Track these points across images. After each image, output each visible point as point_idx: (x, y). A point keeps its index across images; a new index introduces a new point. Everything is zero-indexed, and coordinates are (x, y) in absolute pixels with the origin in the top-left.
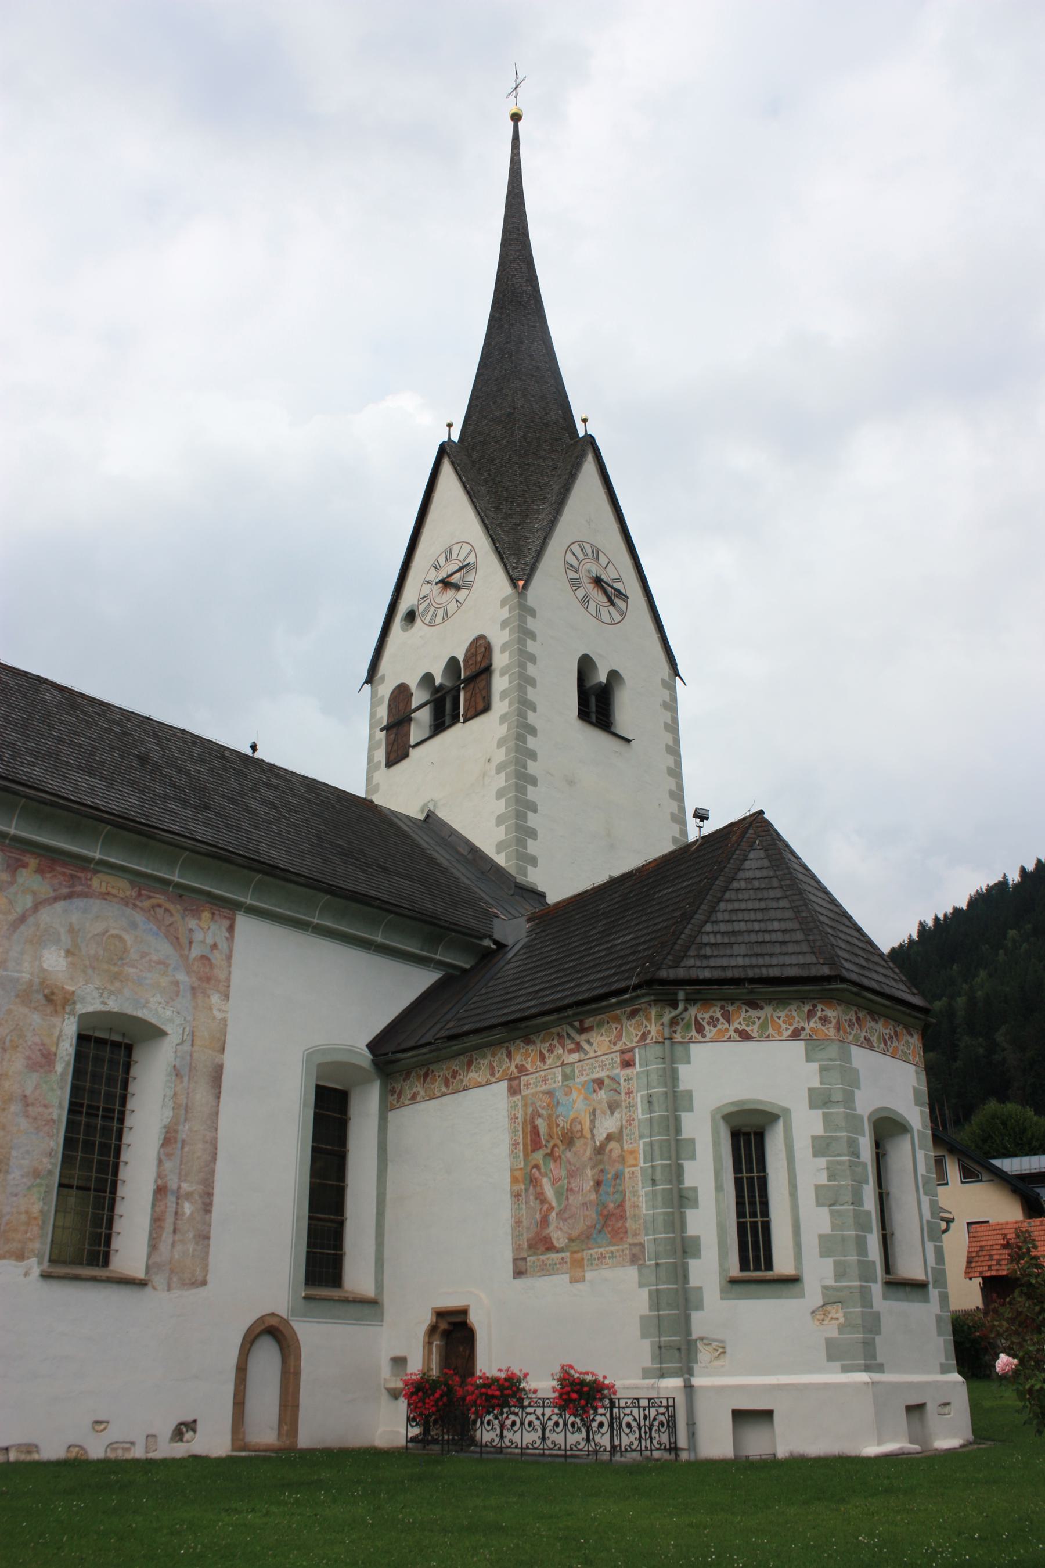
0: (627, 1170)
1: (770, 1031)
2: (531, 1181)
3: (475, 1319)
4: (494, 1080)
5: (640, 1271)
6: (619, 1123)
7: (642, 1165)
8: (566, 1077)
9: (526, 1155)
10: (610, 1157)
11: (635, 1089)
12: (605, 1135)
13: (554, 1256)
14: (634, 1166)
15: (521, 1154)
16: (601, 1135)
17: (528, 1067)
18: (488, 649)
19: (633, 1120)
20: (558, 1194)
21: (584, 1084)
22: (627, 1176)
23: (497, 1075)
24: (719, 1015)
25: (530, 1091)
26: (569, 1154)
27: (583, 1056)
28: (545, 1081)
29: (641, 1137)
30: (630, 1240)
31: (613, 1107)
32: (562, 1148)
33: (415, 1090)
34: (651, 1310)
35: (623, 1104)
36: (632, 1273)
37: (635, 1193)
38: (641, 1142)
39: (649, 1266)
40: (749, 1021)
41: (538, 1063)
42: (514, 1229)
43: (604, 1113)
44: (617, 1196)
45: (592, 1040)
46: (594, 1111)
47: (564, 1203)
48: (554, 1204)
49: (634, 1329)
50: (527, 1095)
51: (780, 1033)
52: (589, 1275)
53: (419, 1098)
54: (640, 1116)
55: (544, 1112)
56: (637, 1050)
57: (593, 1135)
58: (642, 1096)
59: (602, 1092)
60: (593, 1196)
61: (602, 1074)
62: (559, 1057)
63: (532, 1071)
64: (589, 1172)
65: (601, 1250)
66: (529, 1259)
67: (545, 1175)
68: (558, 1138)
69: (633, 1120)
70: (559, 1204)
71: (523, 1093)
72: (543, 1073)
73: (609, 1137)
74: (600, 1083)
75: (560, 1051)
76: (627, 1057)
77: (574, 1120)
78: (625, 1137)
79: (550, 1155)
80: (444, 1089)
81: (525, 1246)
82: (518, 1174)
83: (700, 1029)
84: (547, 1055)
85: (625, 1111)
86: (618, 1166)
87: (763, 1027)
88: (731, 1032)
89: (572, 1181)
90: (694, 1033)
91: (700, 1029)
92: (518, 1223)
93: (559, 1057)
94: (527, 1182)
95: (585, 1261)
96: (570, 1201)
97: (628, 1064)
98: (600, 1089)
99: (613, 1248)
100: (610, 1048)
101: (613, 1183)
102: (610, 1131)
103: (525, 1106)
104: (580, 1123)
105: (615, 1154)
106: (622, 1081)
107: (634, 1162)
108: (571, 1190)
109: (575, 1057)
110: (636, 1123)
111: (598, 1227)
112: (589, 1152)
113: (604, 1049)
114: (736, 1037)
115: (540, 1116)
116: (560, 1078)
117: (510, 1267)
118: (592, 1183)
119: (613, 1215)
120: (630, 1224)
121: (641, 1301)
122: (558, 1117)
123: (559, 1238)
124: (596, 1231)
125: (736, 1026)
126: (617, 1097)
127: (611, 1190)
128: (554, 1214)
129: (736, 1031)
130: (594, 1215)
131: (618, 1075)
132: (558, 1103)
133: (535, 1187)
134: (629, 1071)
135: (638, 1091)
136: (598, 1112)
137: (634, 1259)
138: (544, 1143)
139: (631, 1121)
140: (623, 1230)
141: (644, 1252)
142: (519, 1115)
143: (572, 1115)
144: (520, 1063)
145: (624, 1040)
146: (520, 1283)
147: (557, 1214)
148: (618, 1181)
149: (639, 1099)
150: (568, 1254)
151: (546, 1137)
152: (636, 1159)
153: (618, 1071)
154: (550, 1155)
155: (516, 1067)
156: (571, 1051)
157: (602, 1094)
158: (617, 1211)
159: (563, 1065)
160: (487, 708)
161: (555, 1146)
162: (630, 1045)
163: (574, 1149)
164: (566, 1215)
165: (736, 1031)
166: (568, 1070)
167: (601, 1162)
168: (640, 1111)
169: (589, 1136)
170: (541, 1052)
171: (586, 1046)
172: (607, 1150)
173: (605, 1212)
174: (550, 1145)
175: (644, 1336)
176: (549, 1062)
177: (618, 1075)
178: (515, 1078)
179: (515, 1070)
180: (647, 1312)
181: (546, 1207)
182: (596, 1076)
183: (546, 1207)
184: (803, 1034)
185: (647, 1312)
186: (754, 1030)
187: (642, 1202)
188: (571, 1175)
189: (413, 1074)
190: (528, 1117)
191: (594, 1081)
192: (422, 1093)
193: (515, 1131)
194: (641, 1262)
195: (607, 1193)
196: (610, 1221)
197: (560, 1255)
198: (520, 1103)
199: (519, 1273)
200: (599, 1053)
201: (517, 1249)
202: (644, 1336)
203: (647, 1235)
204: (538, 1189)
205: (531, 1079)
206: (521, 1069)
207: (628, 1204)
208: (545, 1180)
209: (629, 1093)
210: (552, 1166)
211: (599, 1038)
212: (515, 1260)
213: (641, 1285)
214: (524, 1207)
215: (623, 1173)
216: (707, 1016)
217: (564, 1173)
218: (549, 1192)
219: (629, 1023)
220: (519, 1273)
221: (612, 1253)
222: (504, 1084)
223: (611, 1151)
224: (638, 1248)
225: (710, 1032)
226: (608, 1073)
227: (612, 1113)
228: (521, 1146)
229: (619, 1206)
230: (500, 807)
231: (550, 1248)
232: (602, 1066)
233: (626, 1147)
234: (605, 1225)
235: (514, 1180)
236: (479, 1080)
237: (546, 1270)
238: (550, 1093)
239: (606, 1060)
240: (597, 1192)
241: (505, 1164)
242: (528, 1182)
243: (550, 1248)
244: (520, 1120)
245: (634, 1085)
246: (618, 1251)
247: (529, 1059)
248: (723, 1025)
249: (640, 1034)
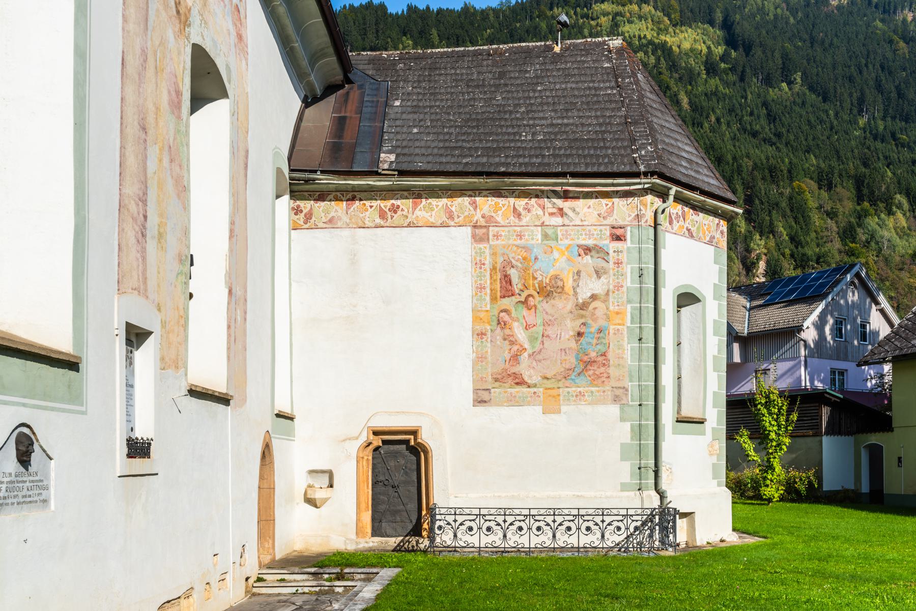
0: (612, 327)
2: (499, 323)
3: (425, 437)
4: (452, 223)
5: (622, 410)
6: (605, 288)
7: (629, 325)
8: (546, 236)
9: (494, 299)
10: (593, 314)
11: (625, 260)
12: (589, 295)
13: (524, 389)
14: (619, 324)
15: (488, 298)
16: (584, 294)
17: (499, 219)
19: (622, 286)
20: (532, 339)
21: (568, 247)
22: (612, 332)
23: (456, 220)
25: (499, 242)
26: (544, 305)
27: (567, 222)
28: (520, 236)
29: (629, 302)
30: (613, 383)
31: (598, 274)
32: (538, 298)
33: (333, 214)
34: (632, 439)
35: (611, 271)
36: (615, 410)
37: (620, 347)
38: (629, 306)
39: (632, 406)
41: (512, 218)
42: (475, 364)
43: (590, 276)
44: (599, 347)
45: (577, 210)
46: (578, 273)
47: (538, 346)
48: (526, 345)
49: (615, 453)
50: (496, 246)
52: (564, 408)
53: (339, 224)
54: (629, 284)
55: (519, 265)
56: (629, 228)
57: (576, 293)
58: (632, 268)
59: (589, 257)
60: (573, 344)
61: (590, 242)
63: (502, 223)
64: (568, 323)
65: (581, 389)
66: (492, 390)
67: (518, 320)
68: (535, 290)
69: (622, 286)
70: (533, 347)
71: (491, 242)
72: (518, 229)
73: (594, 297)
74: (587, 250)
75: (540, 212)
76: (619, 232)
77: (556, 277)
78: (611, 300)
79: (525, 302)
80: (378, 221)
81: (490, 379)
82: (482, 315)
84: (523, 213)
85: (612, 277)
86: (602, 323)
89: (548, 328)
92: (480, 359)
94: (493, 325)
95: (561, 398)
96: (545, 345)
97: (618, 238)
98: (586, 254)
99: (593, 389)
100: (599, 221)
101: (596, 335)
102: (595, 292)
103: (494, 254)
104: (562, 280)
105: (599, 313)
106: (611, 252)
107: (620, 322)
108: (548, 336)
109: (558, 220)
110: (625, 289)
111: (578, 370)
112: (570, 305)
115: (513, 267)
116: (539, 237)
117: (470, 396)
118: (572, 333)
119: (594, 362)
120: (612, 371)
121: (624, 432)
122: (536, 271)
123: (528, 375)
124: (575, 374)
126: (604, 264)
127: (594, 341)
128: (526, 354)
130: (573, 360)
131: (607, 246)
132: (536, 258)
133: (502, 328)
135: (628, 263)
136: (583, 274)
137: (616, 399)
138: (517, 291)
139: (619, 287)
140: (605, 375)
141: (627, 395)
142: (487, 262)
143: (552, 272)
144: (487, 214)
145: (615, 216)
146: (480, 409)
147: (530, 356)
148: (602, 335)
149: (629, 271)
150: (541, 390)
151: (520, 286)
152: (623, 319)
153: (607, 242)
154: (525, 302)
155: (483, 217)
156: (551, 214)
157: (588, 259)
158: (600, 359)
159: (543, 225)
161: (529, 296)
162: (621, 223)
163: (552, 301)
164: (539, 357)
166: (550, 231)
167: (582, 316)
168: (629, 280)
169: (571, 292)
170: (514, 208)
171: (570, 213)
172: (591, 307)
173: (586, 358)
174: (524, 295)
175: (623, 458)
177: (607, 246)
178: (481, 227)
179: (482, 219)
180: (629, 441)
181: (515, 348)
182: (583, 242)
183: (515, 348)
185: (629, 441)
187: (626, 353)
188: (546, 324)
189: (331, 197)
190: (498, 266)
191: (579, 246)
192: (345, 219)
193: (480, 276)
194: (623, 402)
195: (590, 343)
196: (590, 365)
197: (532, 390)
198: (487, 251)
199: (480, 401)
200: (585, 223)
201: (478, 379)
202: (623, 458)
203: (631, 381)
204: (507, 332)
205: (504, 232)
206: (490, 220)
207: (610, 355)
208: (515, 324)
209: (618, 263)
210: (525, 312)
211: (586, 210)
212: (476, 391)
213: (622, 419)
214: (489, 345)
215: (607, 329)
217: (539, 321)
218: (521, 335)
219: (621, 203)
220: (480, 401)
221: (592, 392)
222: (468, 230)
223: (595, 308)
224: (621, 391)
226: (595, 242)
227: (599, 277)
228: (488, 291)
229: (602, 355)
231: (521, 382)
232: (590, 235)
233: (611, 308)
234: (585, 369)
235: (476, 319)
236: (432, 220)
237: (513, 401)
238: (526, 248)
239: (595, 231)
240: (577, 341)
241: (466, 306)
242: (495, 323)
243: (521, 382)
244: (488, 267)
245: (624, 257)
246: (598, 391)
247: (500, 213)
249: (633, 215)
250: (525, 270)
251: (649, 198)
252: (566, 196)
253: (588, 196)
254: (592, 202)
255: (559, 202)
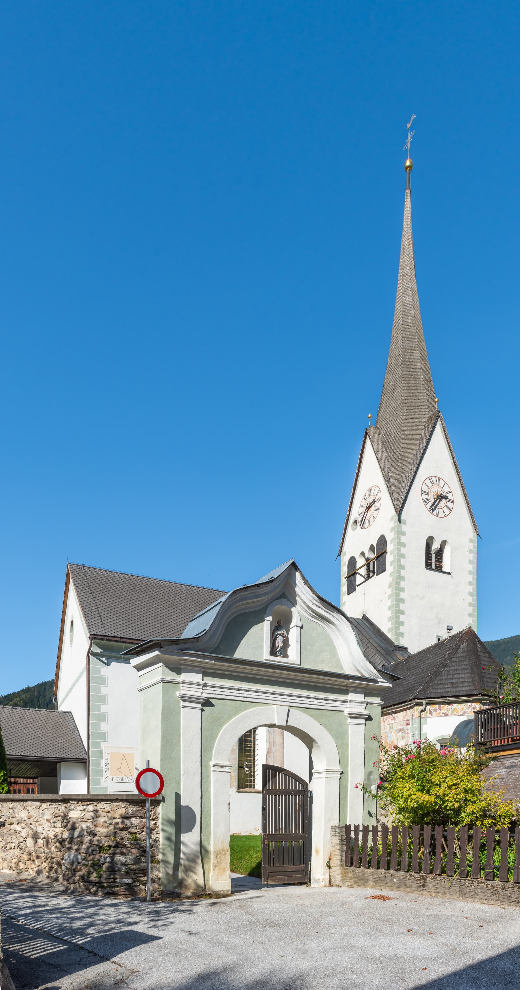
1: (455, 713)
8: (390, 728)
18: (385, 541)
24: (437, 708)
40: (448, 710)
51: (458, 713)
61: (401, 727)
62: (388, 721)
74: (400, 730)
76: (408, 722)
83: (431, 713)
87: (453, 711)
88: (441, 713)
90: (429, 714)
91: (431, 713)
93: (388, 721)
97: (408, 724)
109: (393, 721)
113: (401, 719)
114: (443, 715)
125: (443, 711)
126: (404, 735)
129: (443, 713)
134: (408, 727)
143: (392, 740)
160: (385, 570)
165: (443, 713)
176: (386, 723)
184: (466, 714)
186: (449, 713)
209: (408, 733)
216: (433, 709)
225: (434, 714)
230: (389, 614)
245: (409, 731)
248: (439, 711)
250: (386, 740)
251: (416, 707)
252: (395, 712)
253: (401, 711)
254: (401, 713)
255: (394, 715)
